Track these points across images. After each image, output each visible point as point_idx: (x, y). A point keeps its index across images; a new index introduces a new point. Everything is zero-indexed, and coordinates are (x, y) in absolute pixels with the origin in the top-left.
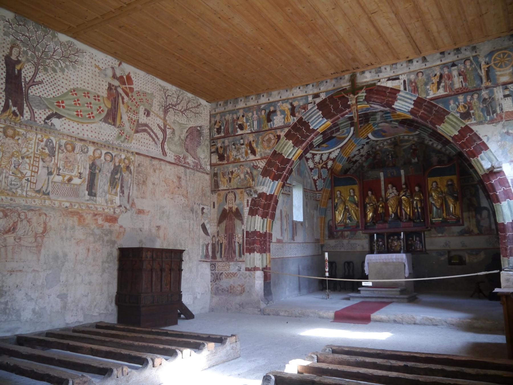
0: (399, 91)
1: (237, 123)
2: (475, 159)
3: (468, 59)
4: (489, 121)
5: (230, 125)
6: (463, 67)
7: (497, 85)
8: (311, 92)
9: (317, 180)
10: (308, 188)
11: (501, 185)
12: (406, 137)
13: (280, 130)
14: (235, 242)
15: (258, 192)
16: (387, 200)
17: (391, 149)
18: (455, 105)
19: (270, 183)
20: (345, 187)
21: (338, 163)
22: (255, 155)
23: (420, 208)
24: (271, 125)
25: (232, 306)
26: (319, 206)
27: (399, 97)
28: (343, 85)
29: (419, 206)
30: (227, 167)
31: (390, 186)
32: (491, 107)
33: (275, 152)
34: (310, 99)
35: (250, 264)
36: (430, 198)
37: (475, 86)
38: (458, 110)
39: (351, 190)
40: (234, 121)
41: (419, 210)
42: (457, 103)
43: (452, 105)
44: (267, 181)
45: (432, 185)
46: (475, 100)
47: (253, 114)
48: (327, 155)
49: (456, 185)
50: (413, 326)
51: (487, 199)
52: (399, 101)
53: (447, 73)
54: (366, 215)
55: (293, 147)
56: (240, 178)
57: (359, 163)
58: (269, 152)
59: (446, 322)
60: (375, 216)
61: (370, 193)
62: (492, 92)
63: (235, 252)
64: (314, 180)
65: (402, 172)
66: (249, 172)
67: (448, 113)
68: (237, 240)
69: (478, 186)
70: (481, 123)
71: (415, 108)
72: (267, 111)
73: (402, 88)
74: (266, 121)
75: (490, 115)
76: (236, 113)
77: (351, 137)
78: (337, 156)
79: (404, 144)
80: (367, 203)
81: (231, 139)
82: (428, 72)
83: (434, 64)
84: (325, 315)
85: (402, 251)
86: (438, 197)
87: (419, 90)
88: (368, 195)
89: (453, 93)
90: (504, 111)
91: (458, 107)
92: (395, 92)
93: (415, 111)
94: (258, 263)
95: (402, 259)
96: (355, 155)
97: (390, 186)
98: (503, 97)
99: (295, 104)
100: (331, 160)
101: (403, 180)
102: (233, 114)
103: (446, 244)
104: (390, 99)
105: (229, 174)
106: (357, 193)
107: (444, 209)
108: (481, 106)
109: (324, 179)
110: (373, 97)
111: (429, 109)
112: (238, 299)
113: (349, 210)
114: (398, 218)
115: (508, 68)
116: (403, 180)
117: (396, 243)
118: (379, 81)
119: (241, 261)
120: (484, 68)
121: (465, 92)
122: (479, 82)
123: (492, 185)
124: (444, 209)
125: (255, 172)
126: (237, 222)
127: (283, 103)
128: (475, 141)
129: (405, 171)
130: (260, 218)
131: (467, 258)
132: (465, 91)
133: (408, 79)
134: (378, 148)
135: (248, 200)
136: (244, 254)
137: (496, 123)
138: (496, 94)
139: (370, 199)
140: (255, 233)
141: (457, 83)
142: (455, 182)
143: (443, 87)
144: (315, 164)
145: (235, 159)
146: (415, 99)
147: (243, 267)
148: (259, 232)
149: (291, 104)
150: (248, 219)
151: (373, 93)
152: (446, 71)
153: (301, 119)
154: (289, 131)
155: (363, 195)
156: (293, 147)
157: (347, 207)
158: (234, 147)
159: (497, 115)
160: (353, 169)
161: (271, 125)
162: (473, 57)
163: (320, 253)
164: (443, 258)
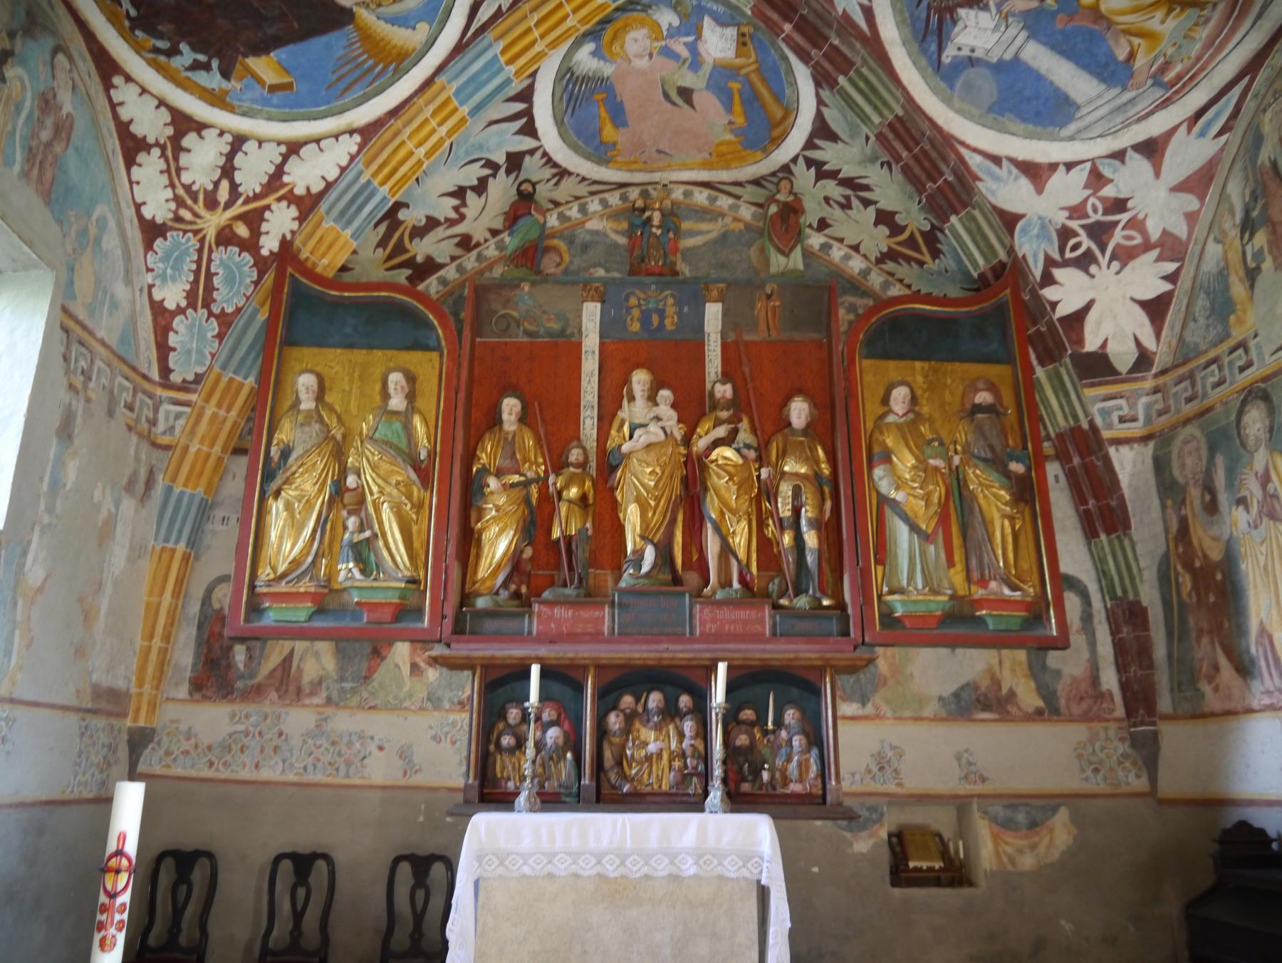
9: (180, 311)
10: (101, 334)
16: (609, 464)
20: (359, 355)
21: (328, 224)
23: (816, 524)
26: (161, 482)
29: (807, 513)
31: (640, 380)
36: (878, 472)
39: (396, 378)
41: (811, 539)
45: (885, 400)
48: (273, 154)
54: (469, 542)
57: (443, 282)
60: (528, 552)
61: (510, 407)
64: (158, 308)
65: (713, 313)
77: (440, 69)
78: (329, 186)
80: (485, 471)
85: (716, 795)
86: (922, 465)
88: (495, 420)
95: (748, 857)
96: (432, 223)
97: (640, 380)
103: (882, 764)
106: (429, 400)
109: (225, 320)
113: (362, 501)
114: (679, 574)
129: (725, 313)
131: (987, 849)
144: (184, 196)
155: (471, 419)
157: (351, 481)
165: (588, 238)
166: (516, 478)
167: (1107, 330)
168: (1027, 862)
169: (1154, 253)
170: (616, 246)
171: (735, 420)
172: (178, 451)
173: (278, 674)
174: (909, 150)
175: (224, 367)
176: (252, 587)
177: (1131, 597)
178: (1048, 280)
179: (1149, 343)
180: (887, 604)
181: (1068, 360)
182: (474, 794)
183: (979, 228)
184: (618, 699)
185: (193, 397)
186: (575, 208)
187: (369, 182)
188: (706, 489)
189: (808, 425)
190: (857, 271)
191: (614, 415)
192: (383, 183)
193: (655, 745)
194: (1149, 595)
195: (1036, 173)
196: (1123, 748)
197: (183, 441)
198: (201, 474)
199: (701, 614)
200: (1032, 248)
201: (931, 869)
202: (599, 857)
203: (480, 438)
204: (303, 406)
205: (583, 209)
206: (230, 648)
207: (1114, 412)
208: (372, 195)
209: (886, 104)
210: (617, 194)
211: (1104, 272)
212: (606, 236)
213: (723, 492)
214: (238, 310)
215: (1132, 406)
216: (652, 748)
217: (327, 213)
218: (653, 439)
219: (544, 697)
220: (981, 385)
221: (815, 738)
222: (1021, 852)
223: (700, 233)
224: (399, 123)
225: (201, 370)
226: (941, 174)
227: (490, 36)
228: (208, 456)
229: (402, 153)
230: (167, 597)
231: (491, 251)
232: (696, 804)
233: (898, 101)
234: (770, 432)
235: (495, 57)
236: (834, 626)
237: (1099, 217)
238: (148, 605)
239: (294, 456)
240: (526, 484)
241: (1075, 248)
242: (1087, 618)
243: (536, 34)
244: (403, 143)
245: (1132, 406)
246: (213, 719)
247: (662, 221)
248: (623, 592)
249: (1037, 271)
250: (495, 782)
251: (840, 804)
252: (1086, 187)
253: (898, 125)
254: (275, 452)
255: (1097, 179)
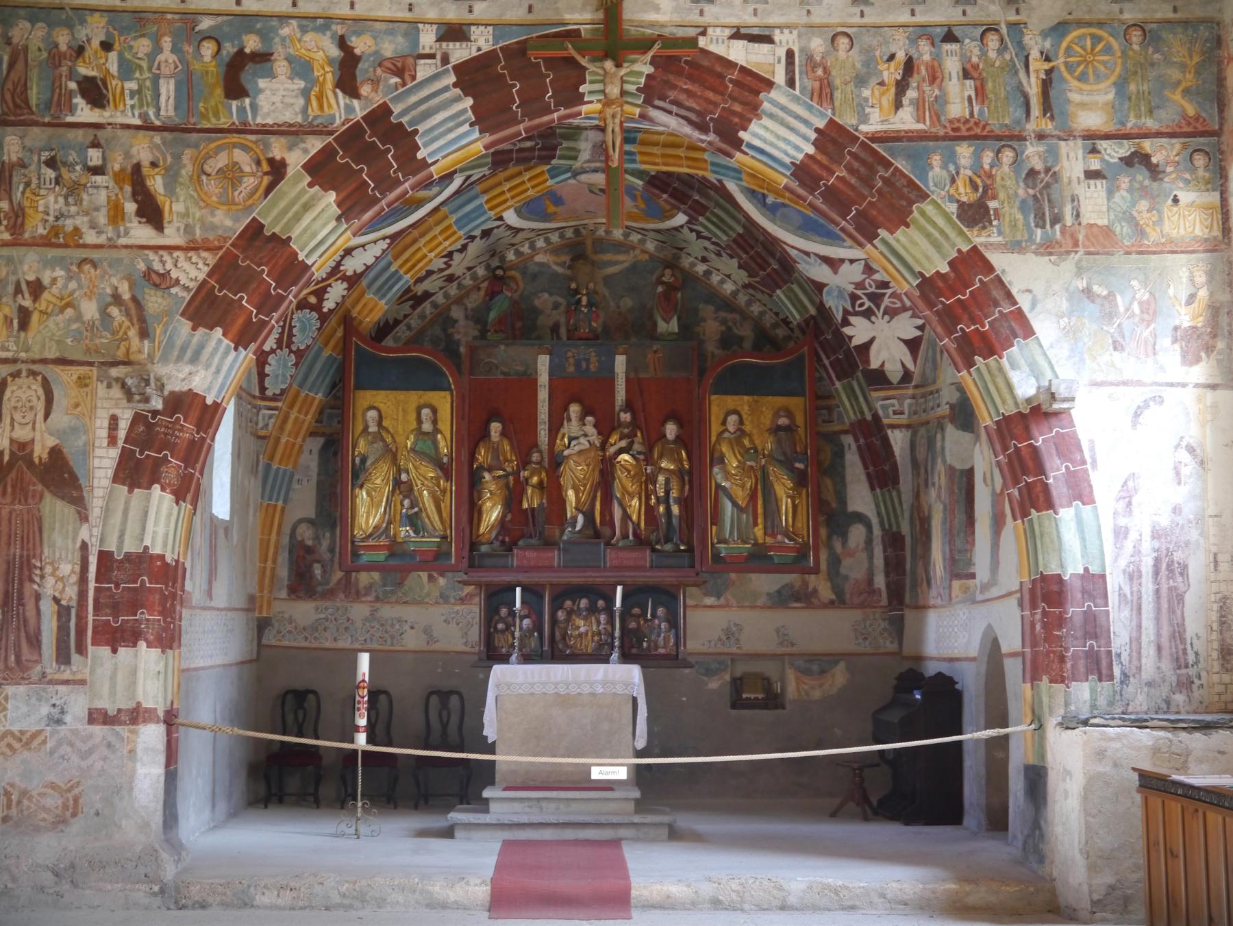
0: (770, 84)
1: (72, 75)
2: (991, 360)
3: (991, 28)
4: (1041, 245)
5: (34, 75)
6: (976, 51)
7: (1069, 135)
8: (432, 14)
9: (273, 351)
11: (1063, 455)
12: (618, 234)
13: (283, 140)
14: (38, 597)
15: (169, 388)
16: (556, 461)
17: (559, 270)
18: (944, 173)
19: (226, 353)
20: (401, 395)
21: (369, 296)
22: (159, 226)
23: (679, 501)
24: (242, 110)
25: (14, 879)
27: (766, 106)
28: (568, 17)
29: (674, 494)
30: (9, 260)
31: (574, 409)
32: (1049, 201)
33: (255, 229)
34: (427, 39)
35: (113, 692)
36: (716, 470)
37: (1007, 122)
38: (952, 191)
40: (55, 57)
41: (675, 510)
42: (952, 168)
43: (937, 171)
44: (213, 343)
45: (724, 423)
46: (1006, 168)
47: (158, 49)
49: (801, 431)
50: (783, 916)
51: (872, 488)
52: (766, 121)
53: (927, 57)
54: (473, 511)
55: (338, 219)
56: (79, 317)
57: (435, 305)
58: (229, 224)
59: (883, 896)
60: (509, 517)
61: (495, 427)
62: (1053, 153)
63: (35, 642)
65: (620, 361)
66: (126, 296)
67: (924, 196)
68: (49, 587)
69: (848, 440)
70: (1015, 247)
71: (819, 157)
72: (229, 49)
73: (780, 77)
74: (219, 91)
75: (1043, 227)
76: (69, 25)
77: (443, 203)
79: (607, 257)
80: (481, 468)
81: (37, 135)
82: (868, 39)
83: (891, 19)
84: (452, 896)
85: (615, 656)
86: (741, 466)
87: (838, 95)
88: (485, 435)
89: (941, 133)
90: (1084, 221)
91: (953, 181)
92: (753, 85)
93: (815, 167)
94: (152, 694)
95: (628, 684)
96: (430, 273)
97: (574, 409)
98: (1082, 176)
99: (361, 45)
100: (344, 278)
101: (620, 395)
102: (51, 25)
103: (728, 634)
104: (737, 108)
105: (18, 290)
107: (760, 511)
108: (1021, 192)
109: (299, 354)
110: (674, 87)
111: (862, 170)
112: (48, 847)
113: (411, 490)
114: (596, 533)
115: (1102, 86)
116: (620, 395)
117: (582, 625)
118: (704, 33)
119: (66, 682)
120: (1037, 71)
121: (976, 137)
122: (1020, 113)
123: (1035, 451)
124: (760, 511)
125: (154, 302)
126: (54, 509)
127: (304, 30)
128: (996, 304)
129: (628, 362)
130: (169, 497)
131: (793, 686)
132: (978, 131)
133: (802, 50)
134: (511, 256)
135: (114, 420)
136: (81, 650)
137: (1060, 254)
138: (1065, 163)
139: (496, 451)
140: (142, 561)
141: (958, 100)
142: (800, 420)
143: (911, 102)
145: (56, 231)
146: (821, 124)
147: (78, 705)
148: (162, 557)
149: (342, 43)
150: (110, 497)
151: (679, 73)
152: (925, 52)
153: (385, 110)
154: (326, 154)
155: (472, 434)
156: (338, 219)
158: (50, 174)
159: (1063, 232)
160: (409, 327)
161: (242, 110)
162: (1011, 25)
163: (254, 656)
164: (713, 684)
165: (536, 269)
166: (501, 473)
167: (884, 356)
168: (817, 694)
169: (910, 313)
170: (556, 274)
171: (632, 436)
172: (272, 440)
173: (344, 582)
174: (746, 253)
175: (301, 385)
176: (353, 542)
177: (895, 529)
178: (846, 323)
179: (910, 365)
180: (718, 549)
181: (859, 374)
182: (484, 656)
183: (796, 296)
184: (563, 603)
185: (280, 404)
186: (527, 245)
187: (397, 271)
188: (614, 478)
189: (677, 437)
190: (729, 292)
191: (559, 430)
192: (406, 273)
193: (583, 627)
194: (905, 529)
195: (833, 264)
196: (884, 624)
197: (274, 433)
198: (290, 456)
199: (610, 554)
200: (835, 305)
201: (756, 699)
202: (556, 684)
203: (476, 445)
204: (370, 430)
205: (532, 246)
206: (311, 566)
207: (889, 407)
208: (400, 279)
209: (731, 228)
210: (557, 234)
211: (880, 321)
212: (549, 267)
213: (624, 482)
214: (308, 347)
215: (901, 404)
216: (582, 630)
217: (370, 286)
218: (582, 447)
219: (523, 602)
220: (782, 413)
221: (673, 623)
222: (813, 688)
223: (617, 263)
224: (416, 233)
225: (284, 387)
226: (769, 265)
227: (478, 188)
228: (294, 444)
229: (419, 255)
230: (274, 536)
231: (468, 282)
232: (606, 660)
233: (738, 222)
234: (654, 438)
235: (481, 205)
236: (686, 562)
237: (873, 290)
238: (262, 540)
239: (369, 463)
240: (506, 476)
241: (861, 305)
242: (869, 541)
243: (508, 195)
244: (419, 249)
245: (901, 404)
246: (304, 611)
247: (589, 301)
248: (565, 542)
249: (839, 317)
250: (495, 649)
251: (685, 660)
252: (863, 273)
253: (740, 240)
254: (357, 460)
255: (869, 270)
